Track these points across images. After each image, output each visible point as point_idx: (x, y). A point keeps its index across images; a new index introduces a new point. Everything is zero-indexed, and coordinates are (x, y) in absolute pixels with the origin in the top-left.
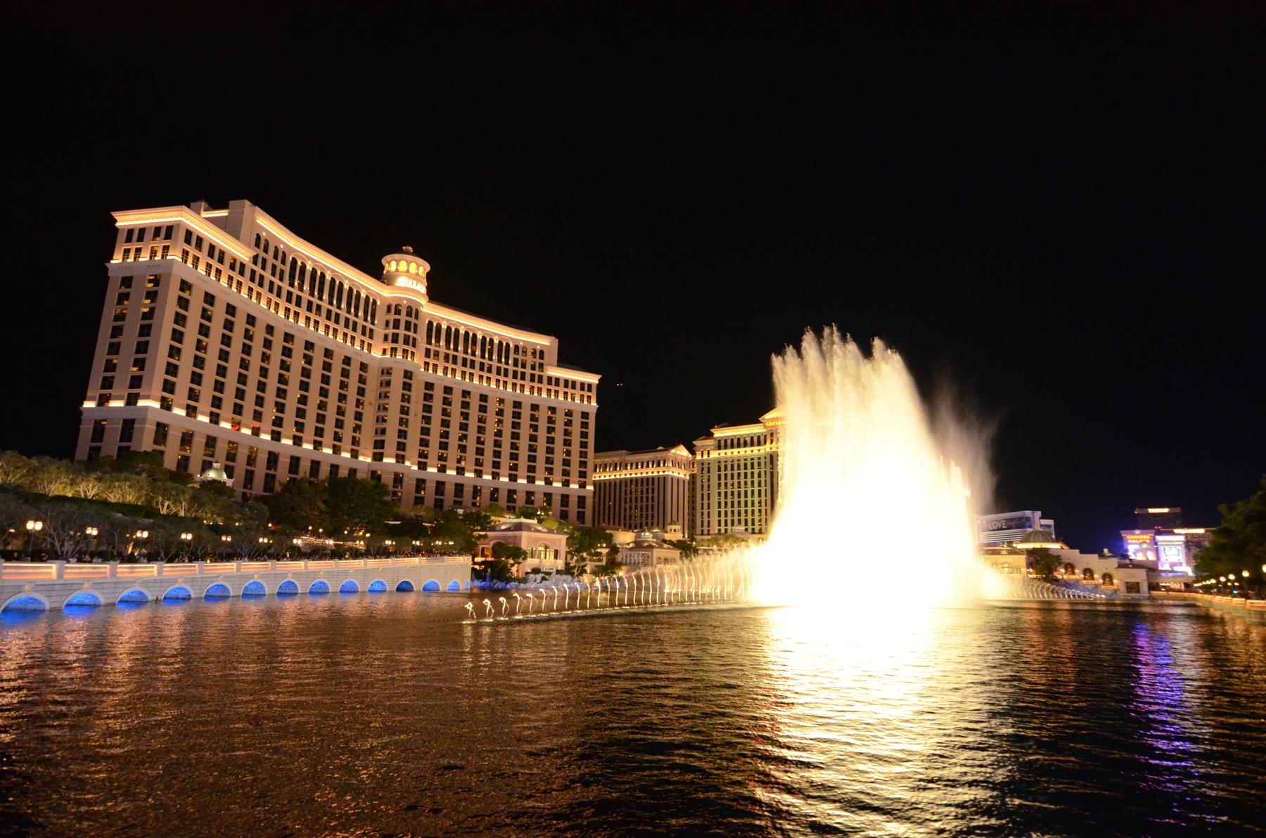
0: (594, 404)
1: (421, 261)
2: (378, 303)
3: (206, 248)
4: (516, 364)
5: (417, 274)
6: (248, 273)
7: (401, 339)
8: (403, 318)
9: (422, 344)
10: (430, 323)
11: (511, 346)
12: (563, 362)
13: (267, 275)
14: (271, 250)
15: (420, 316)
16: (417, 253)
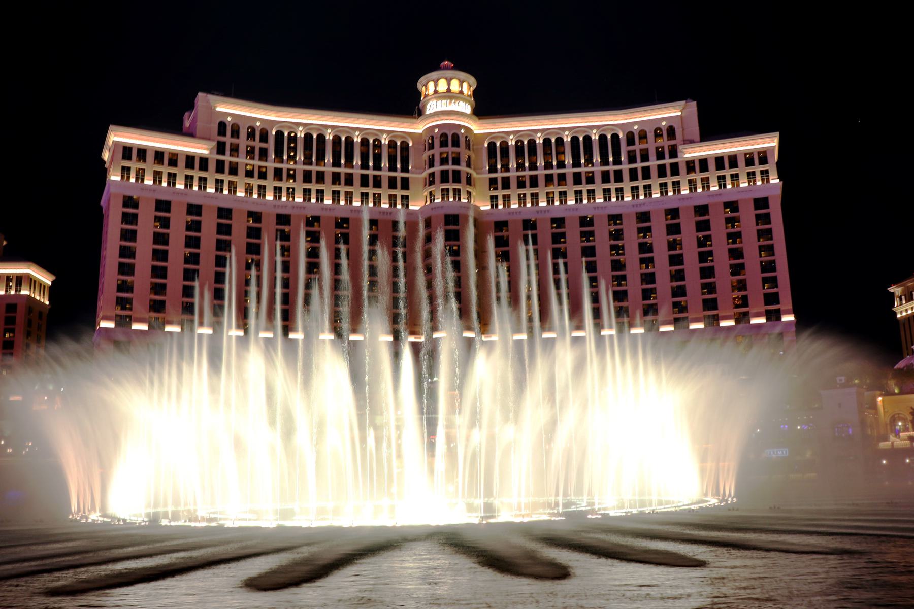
0: (778, 181)
1: (463, 75)
2: (411, 144)
3: (150, 157)
4: (632, 159)
5: (449, 90)
6: (212, 166)
7: (438, 178)
8: (437, 151)
9: (482, 176)
10: (492, 145)
11: (621, 136)
12: (708, 133)
13: (242, 160)
14: (243, 133)
15: (462, 141)
16: (459, 67)
